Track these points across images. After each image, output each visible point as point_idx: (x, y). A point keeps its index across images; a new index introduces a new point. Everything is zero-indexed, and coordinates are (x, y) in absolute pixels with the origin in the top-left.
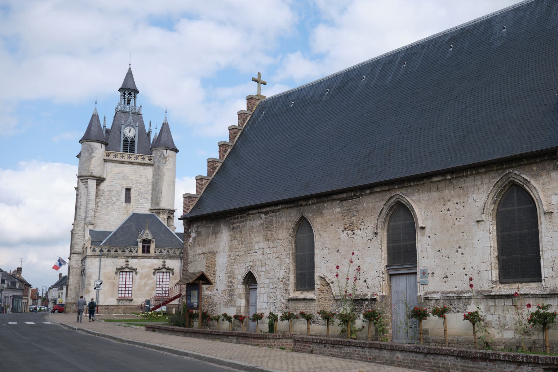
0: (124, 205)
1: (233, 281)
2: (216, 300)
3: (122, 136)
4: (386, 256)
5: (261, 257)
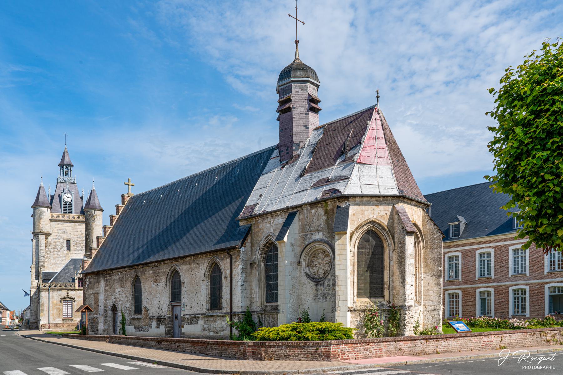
0: (66, 252)
5: (119, 296)
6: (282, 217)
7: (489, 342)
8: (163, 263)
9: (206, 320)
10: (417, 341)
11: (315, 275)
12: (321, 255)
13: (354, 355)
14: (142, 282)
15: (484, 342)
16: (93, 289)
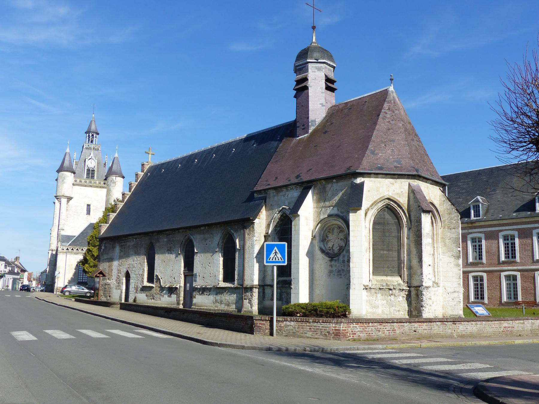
1: (120, 275)
2: (112, 286)
3: (86, 166)
4: (183, 265)
6: (297, 191)
7: (510, 328)
8: (177, 231)
9: (218, 291)
10: (432, 324)
11: (329, 250)
12: (336, 230)
13: (366, 335)
14: (156, 249)
15: (504, 327)
16: (108, 254)
